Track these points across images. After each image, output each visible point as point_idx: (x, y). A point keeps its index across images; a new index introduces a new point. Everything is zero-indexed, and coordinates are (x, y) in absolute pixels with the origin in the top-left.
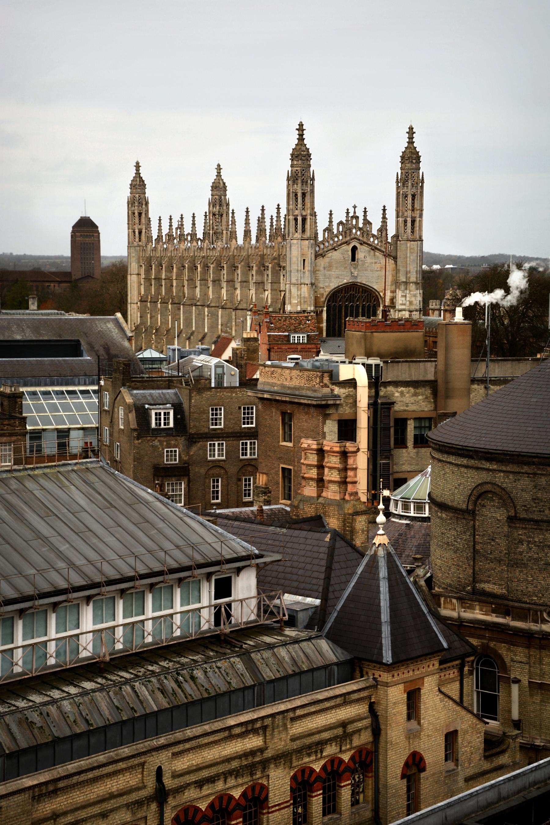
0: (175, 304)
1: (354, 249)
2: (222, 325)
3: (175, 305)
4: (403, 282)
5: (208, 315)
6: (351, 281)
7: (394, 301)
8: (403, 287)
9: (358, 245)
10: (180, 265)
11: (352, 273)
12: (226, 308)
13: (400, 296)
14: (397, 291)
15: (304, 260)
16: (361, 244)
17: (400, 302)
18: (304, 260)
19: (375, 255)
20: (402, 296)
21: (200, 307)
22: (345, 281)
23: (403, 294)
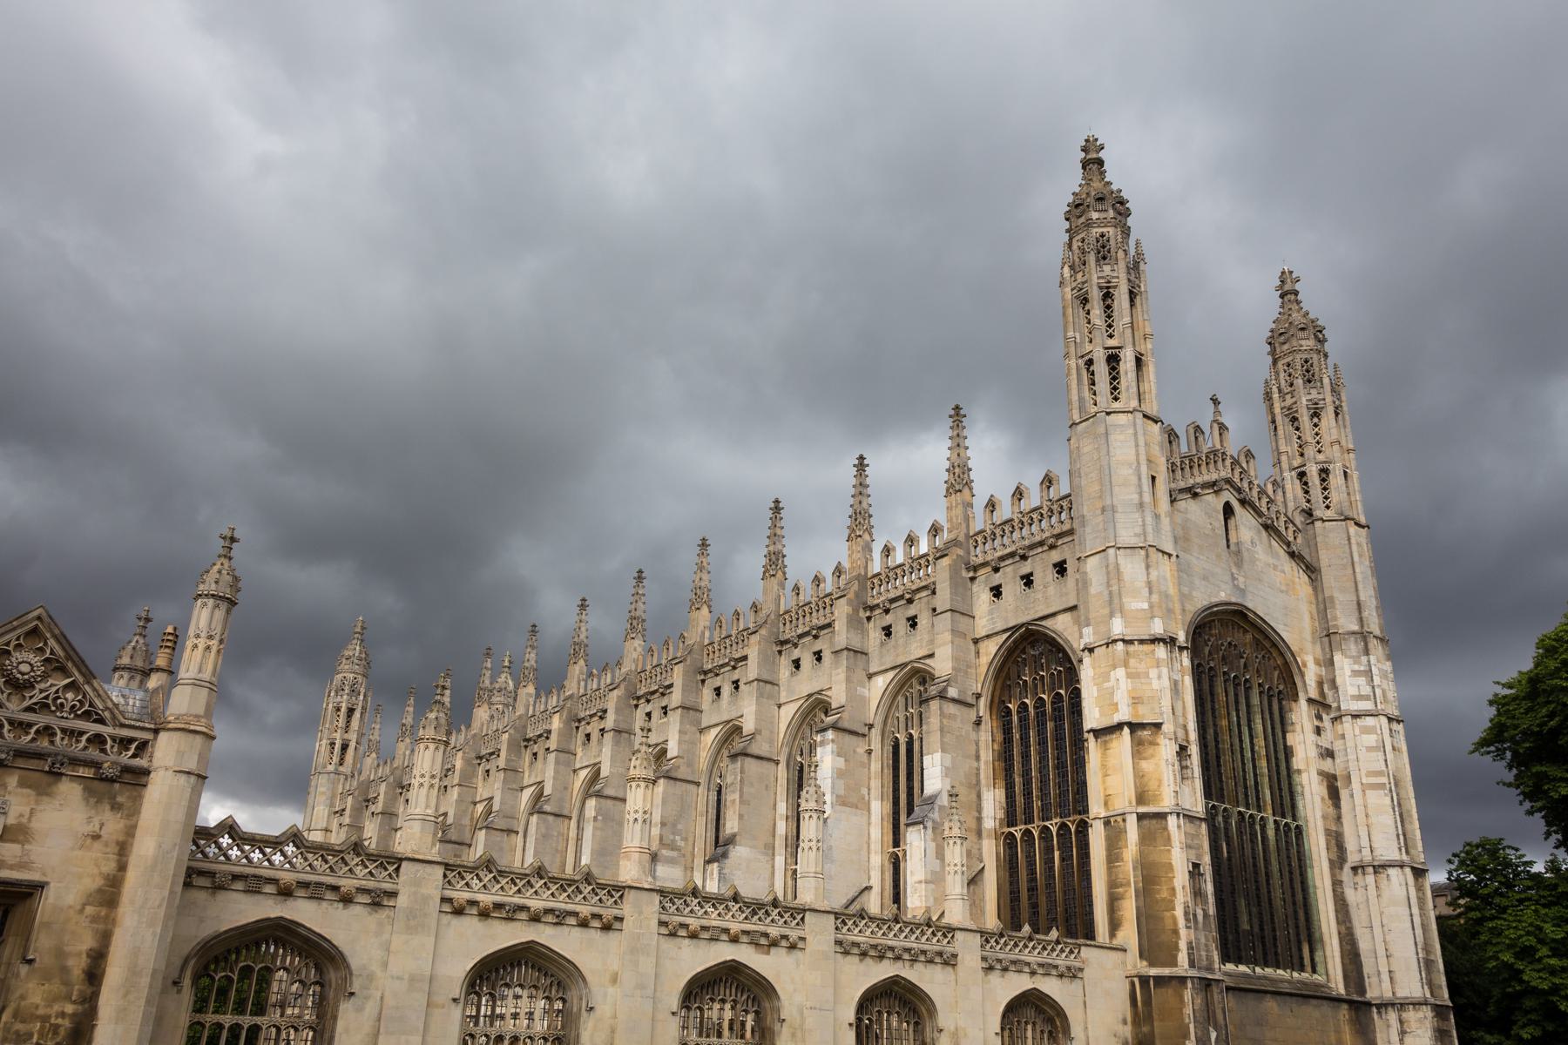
0: (450, 842)
1: (1228, 511)
2: (663, 824)
3: (450, 846)
4: (1354, 633)
5: (595, 818)
6: (1233, 600)
7: (1326, 687)
8: (1353, 647)
9: (1236, 505)
10: (474, 755)
11: (1234, 579)
12: (675, 779)
13: (1348, 673)
14: (1338, 658)
15: (1153, 478)
16: (1243, 502)
17: (1352, 691)
18: (1153, 478)
19: (1270, 546)
20: (1356, 673)
21: (551, 818)
22: (1223, 596)
23: (1356, 667)
